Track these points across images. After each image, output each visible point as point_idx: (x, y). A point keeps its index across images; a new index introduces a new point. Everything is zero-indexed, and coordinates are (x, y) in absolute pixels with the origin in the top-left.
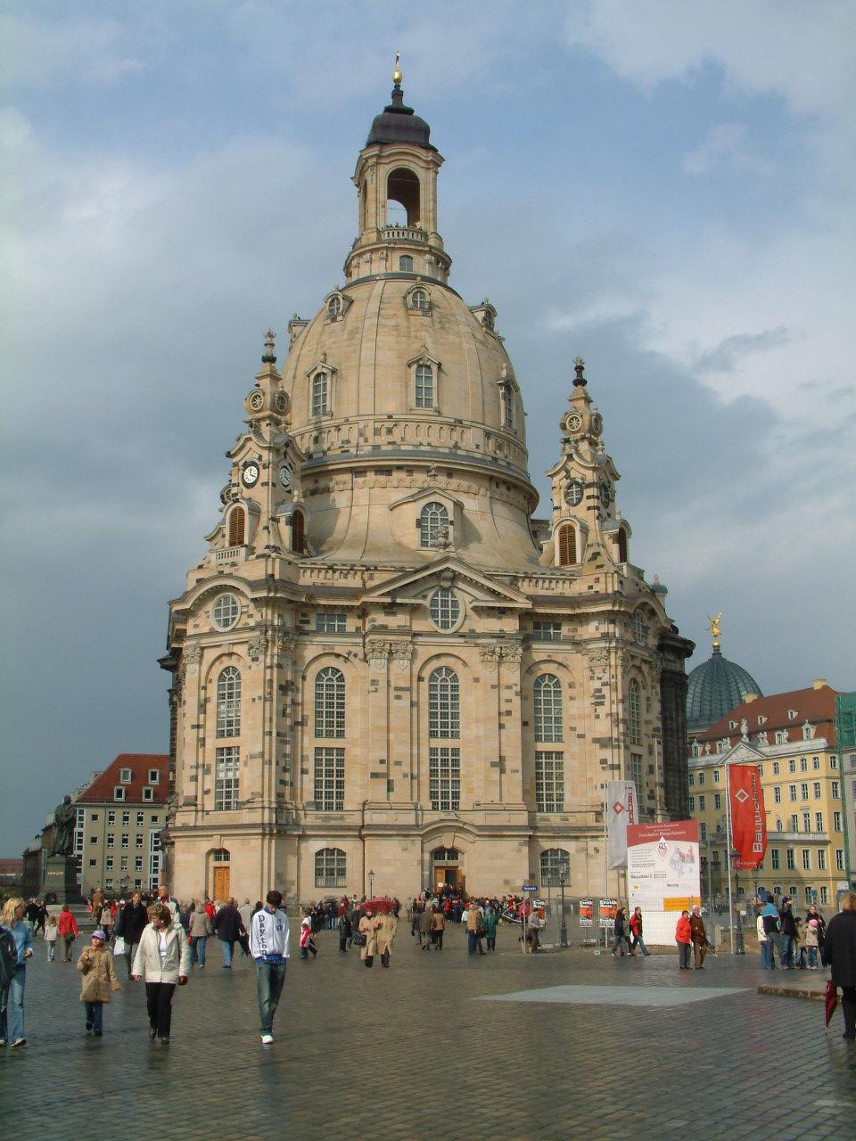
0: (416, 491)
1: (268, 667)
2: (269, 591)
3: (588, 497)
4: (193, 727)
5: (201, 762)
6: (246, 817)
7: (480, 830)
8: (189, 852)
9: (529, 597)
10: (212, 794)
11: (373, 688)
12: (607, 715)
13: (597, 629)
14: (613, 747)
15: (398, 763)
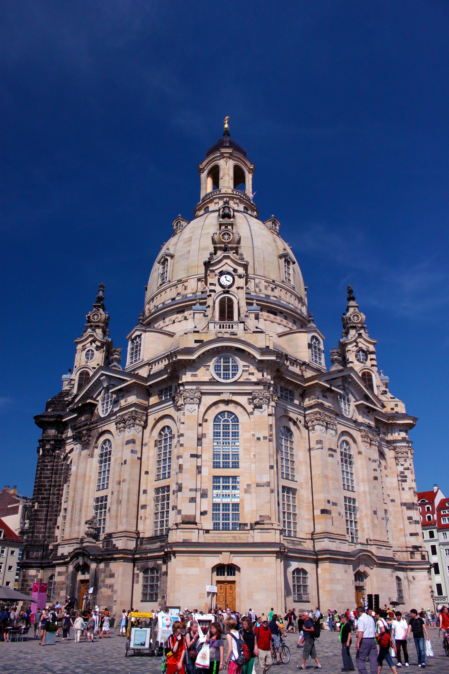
0: (288, 329)
1: (269, 415)
2: (276, 357)
3: (371, 359)
4: (192, 456)
5: (199, 487)
6: (258, 537)
7: (379, 560)
8: (191, 566)
9: (383, 406)
10: (209, 515)
11: (319, 446)
12: (410, 489)
13: (399, 434)
14: (417, 509)
15: (334, 504)
